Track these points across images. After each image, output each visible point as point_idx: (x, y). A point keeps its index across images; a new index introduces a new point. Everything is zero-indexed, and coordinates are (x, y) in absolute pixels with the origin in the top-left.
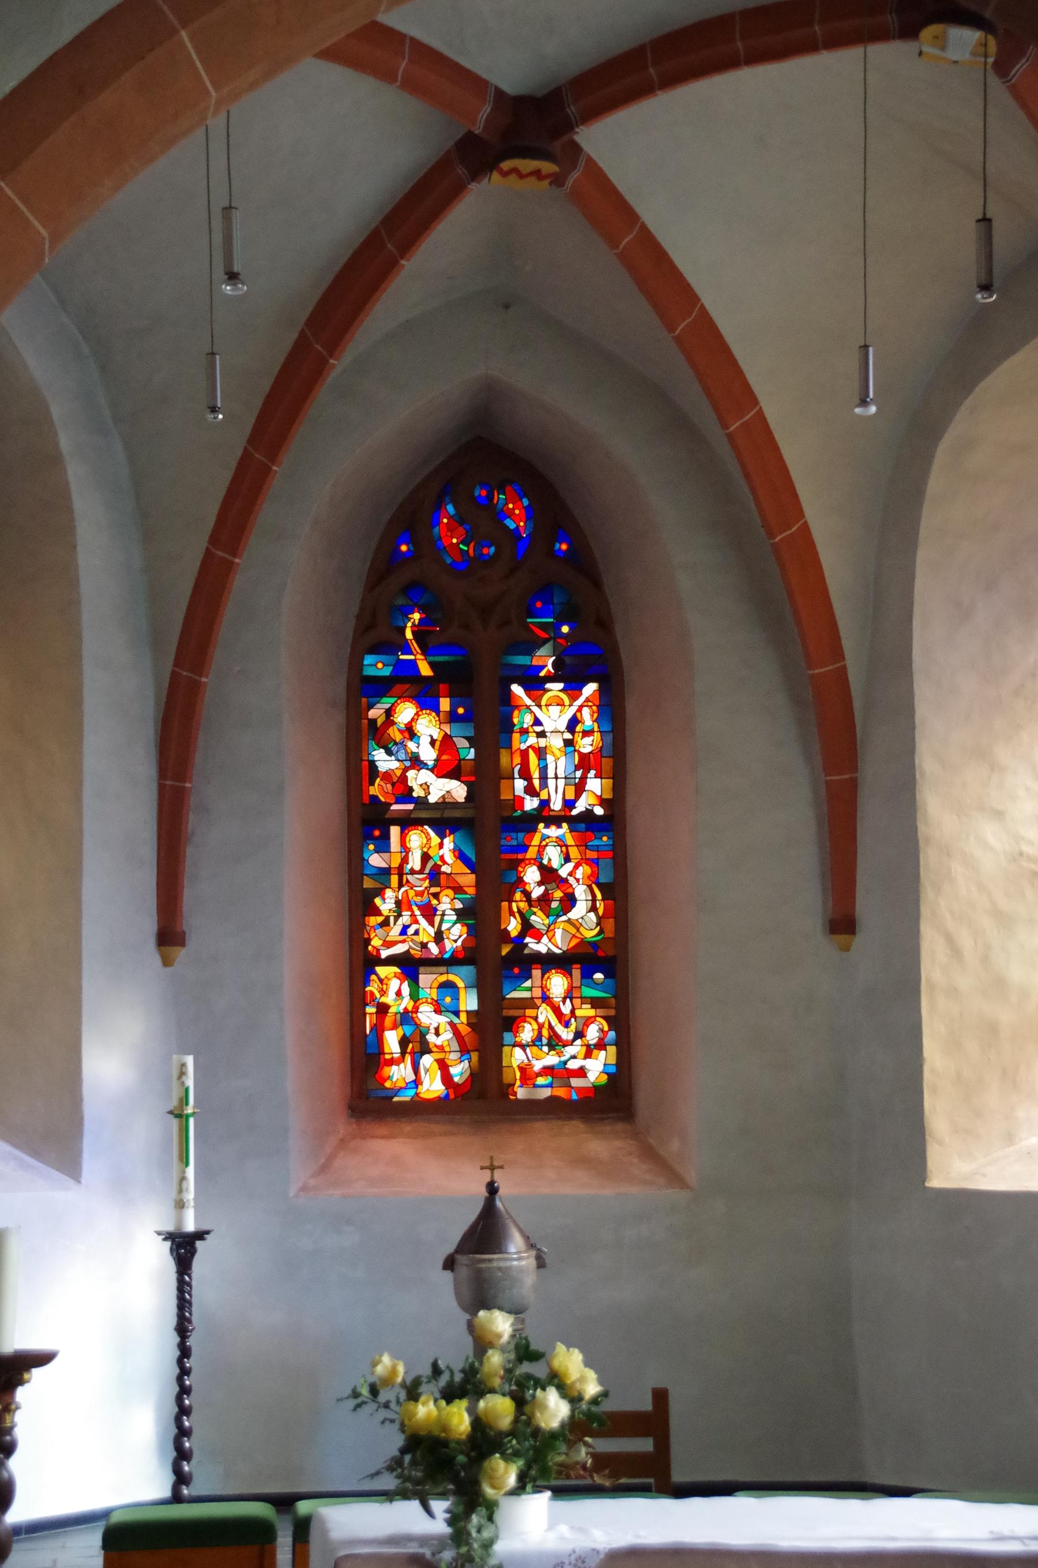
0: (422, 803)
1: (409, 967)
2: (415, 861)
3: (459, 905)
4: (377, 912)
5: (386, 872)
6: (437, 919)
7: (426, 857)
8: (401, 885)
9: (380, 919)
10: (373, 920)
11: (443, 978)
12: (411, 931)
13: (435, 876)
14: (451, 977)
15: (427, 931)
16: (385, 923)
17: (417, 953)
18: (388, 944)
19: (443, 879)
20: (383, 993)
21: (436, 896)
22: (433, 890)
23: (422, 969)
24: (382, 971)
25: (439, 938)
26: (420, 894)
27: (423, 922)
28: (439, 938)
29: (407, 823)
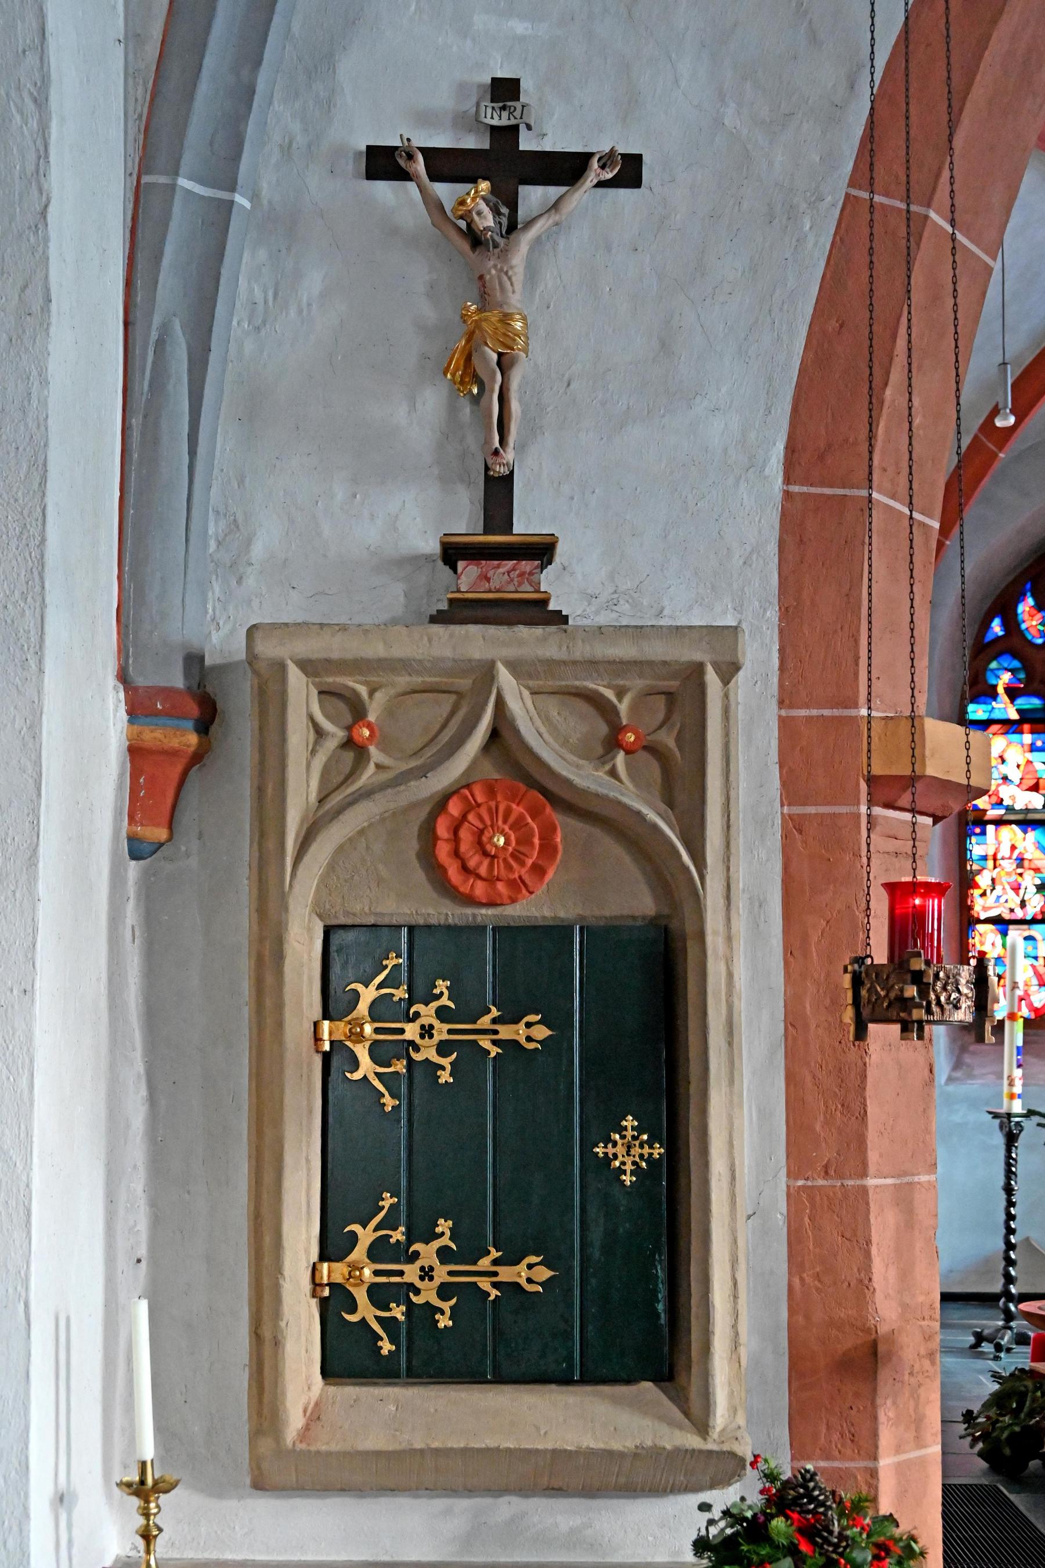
0: (1010, 809)
1: (1001, 923)
2: (1005, 851)
3: (1039, 882)
4: (977, 886)
5: (985, 858)
6: (1022, 892)
7: (1013, 848)
8: (995, 867)
9: (980, 891)
10: (976, 893)
11: (1026, 934)
12: (1002, 900)
13: (1021, 861)
14: (1032, 933)
15: (1014, 900)
16: (983, 894)
17: (1007, 916)
18: (985, 909)
19: (1026, 864)
20: (982, 943)
21: (1021, 875)
22: (1020, 871)
23: (1011, 927)
24: (980, 927)
25: (1023, 904)
26: (1009, 874)
27: (1011, 894)
28: (1023, 904)
29: (999, 822)
